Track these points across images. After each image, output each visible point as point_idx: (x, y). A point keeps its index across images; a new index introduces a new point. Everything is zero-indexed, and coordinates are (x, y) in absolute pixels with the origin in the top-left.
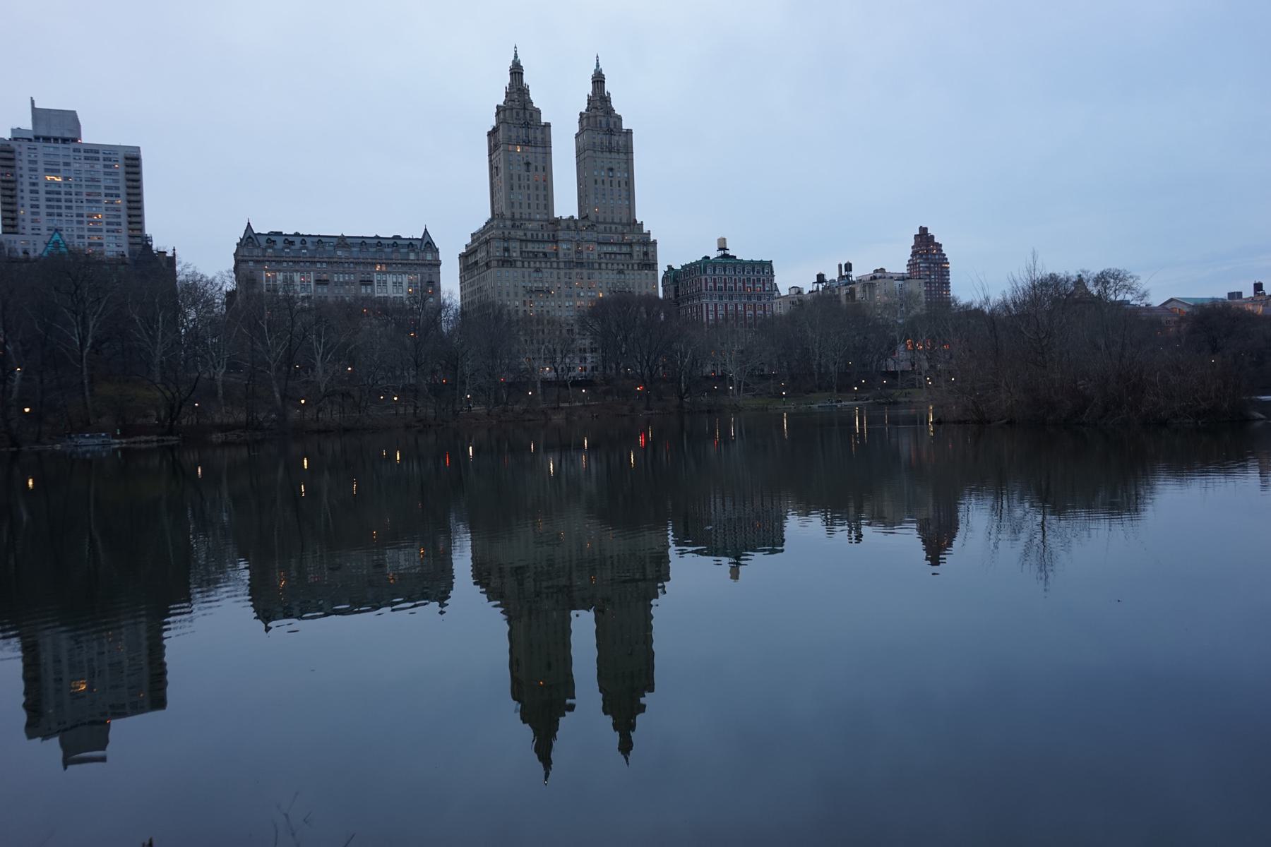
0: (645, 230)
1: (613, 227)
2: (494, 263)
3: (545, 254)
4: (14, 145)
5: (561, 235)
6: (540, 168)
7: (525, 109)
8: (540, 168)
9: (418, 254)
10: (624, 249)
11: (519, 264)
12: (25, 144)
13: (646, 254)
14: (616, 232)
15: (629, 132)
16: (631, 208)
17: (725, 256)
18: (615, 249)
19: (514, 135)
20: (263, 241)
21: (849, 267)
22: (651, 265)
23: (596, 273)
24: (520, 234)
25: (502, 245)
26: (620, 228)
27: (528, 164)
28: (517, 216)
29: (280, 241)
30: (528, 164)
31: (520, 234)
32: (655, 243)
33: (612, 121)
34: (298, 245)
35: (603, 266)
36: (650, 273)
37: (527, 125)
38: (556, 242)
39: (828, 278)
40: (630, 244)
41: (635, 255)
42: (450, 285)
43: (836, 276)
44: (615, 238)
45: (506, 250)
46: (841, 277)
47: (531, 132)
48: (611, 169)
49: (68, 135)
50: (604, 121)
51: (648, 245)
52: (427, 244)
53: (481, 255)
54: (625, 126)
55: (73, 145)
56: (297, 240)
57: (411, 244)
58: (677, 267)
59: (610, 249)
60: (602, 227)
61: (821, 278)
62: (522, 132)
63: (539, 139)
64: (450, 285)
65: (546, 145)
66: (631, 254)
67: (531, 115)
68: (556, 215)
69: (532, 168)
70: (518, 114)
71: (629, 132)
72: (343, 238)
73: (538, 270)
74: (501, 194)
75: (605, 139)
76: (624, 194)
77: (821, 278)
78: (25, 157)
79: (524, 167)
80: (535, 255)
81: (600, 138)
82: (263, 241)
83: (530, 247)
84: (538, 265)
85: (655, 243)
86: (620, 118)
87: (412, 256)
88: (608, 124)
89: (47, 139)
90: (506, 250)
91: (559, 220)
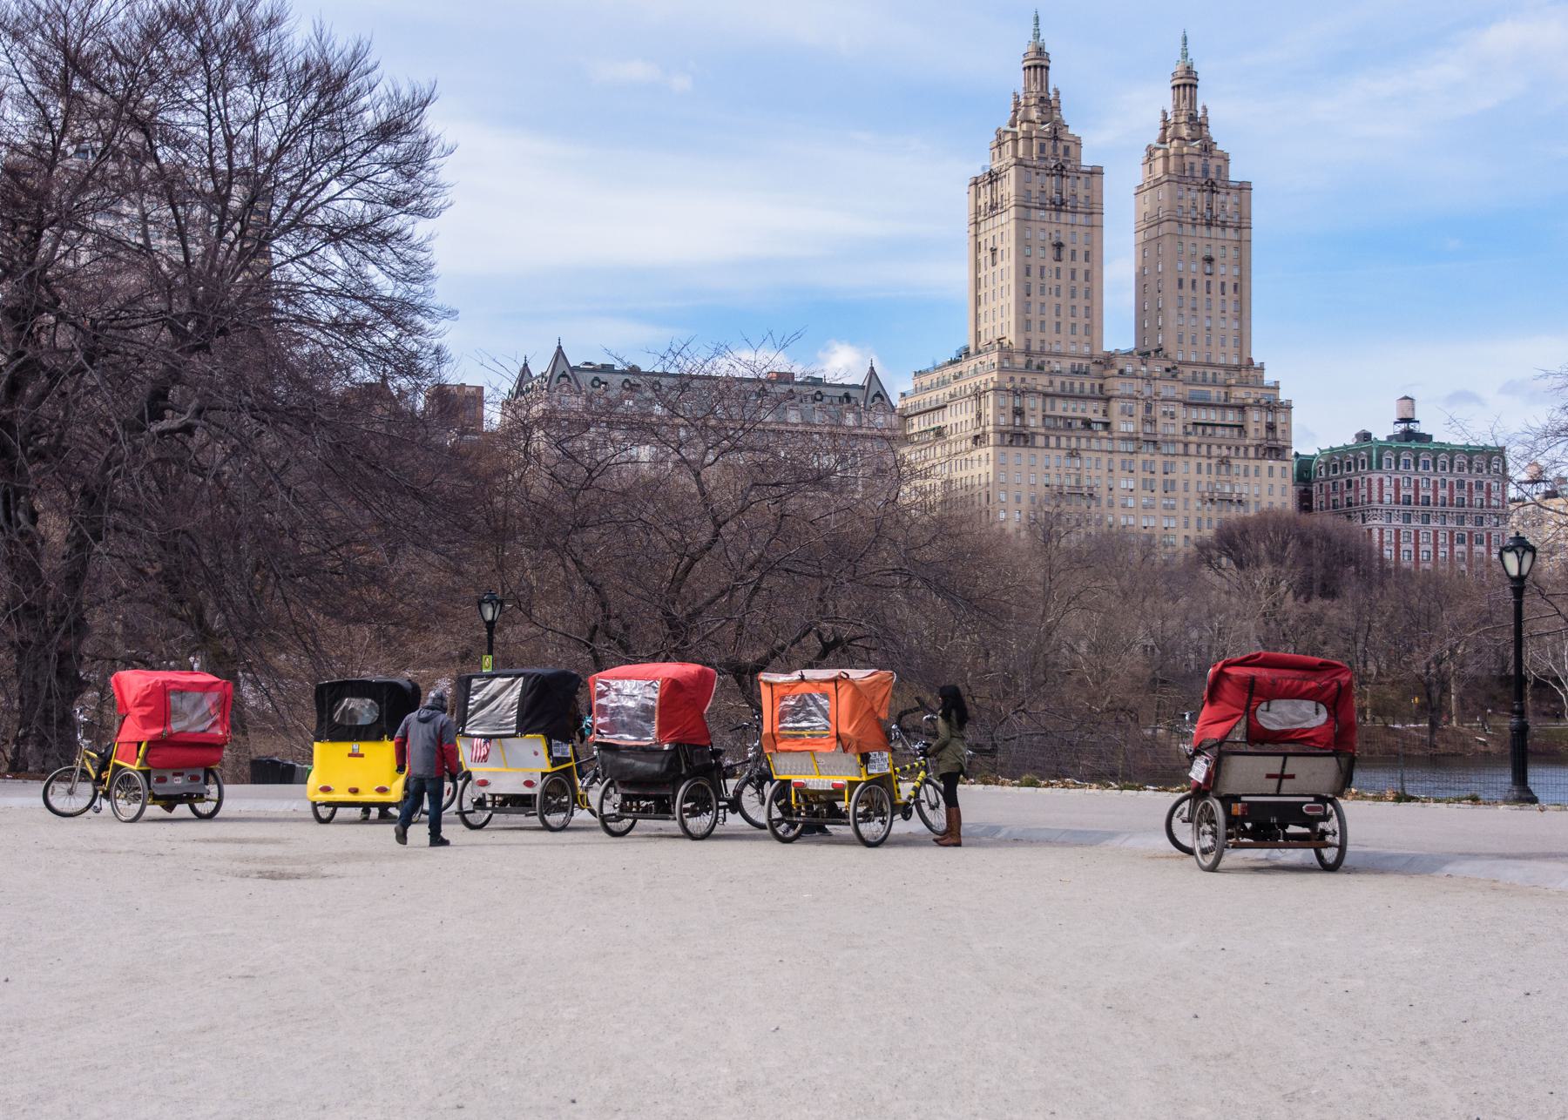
0: (1269, 378)
1: (1210, 372)
3: (1087, 424)
5: (1117, 386)
6: (1080, 256)
7: (1056, 138)
8: (1080, 256)
11: (1040, 441)
13: (1271, 427)
14: (1214, 383)
16: (1242, 340)
23: (1180, 461)
26: (1222, 375)
27: (1059, 246)
28: (1035, 347)
30: (1059, 246)
32: (1288, 407)
33: (1213, 163)
35: (1192, 449)
37: (1060, 171)
38: (1108, 399)
40: (1241, 408)
41: (1251, 429)
45: (1019, 412)
48: (1209, 260)
62: (1051, 183)
63: (1081, 198)
65: (1093, 210)
67: (1067, 149)
69: (1066, 254)
73: (1073, 454)
76: (1230, 308)
79: (1051, 252)
84: (1074, 443)
87: (850, 419)
88: (1206, 171)
90: (1019, 412)
91: (1108, 361)
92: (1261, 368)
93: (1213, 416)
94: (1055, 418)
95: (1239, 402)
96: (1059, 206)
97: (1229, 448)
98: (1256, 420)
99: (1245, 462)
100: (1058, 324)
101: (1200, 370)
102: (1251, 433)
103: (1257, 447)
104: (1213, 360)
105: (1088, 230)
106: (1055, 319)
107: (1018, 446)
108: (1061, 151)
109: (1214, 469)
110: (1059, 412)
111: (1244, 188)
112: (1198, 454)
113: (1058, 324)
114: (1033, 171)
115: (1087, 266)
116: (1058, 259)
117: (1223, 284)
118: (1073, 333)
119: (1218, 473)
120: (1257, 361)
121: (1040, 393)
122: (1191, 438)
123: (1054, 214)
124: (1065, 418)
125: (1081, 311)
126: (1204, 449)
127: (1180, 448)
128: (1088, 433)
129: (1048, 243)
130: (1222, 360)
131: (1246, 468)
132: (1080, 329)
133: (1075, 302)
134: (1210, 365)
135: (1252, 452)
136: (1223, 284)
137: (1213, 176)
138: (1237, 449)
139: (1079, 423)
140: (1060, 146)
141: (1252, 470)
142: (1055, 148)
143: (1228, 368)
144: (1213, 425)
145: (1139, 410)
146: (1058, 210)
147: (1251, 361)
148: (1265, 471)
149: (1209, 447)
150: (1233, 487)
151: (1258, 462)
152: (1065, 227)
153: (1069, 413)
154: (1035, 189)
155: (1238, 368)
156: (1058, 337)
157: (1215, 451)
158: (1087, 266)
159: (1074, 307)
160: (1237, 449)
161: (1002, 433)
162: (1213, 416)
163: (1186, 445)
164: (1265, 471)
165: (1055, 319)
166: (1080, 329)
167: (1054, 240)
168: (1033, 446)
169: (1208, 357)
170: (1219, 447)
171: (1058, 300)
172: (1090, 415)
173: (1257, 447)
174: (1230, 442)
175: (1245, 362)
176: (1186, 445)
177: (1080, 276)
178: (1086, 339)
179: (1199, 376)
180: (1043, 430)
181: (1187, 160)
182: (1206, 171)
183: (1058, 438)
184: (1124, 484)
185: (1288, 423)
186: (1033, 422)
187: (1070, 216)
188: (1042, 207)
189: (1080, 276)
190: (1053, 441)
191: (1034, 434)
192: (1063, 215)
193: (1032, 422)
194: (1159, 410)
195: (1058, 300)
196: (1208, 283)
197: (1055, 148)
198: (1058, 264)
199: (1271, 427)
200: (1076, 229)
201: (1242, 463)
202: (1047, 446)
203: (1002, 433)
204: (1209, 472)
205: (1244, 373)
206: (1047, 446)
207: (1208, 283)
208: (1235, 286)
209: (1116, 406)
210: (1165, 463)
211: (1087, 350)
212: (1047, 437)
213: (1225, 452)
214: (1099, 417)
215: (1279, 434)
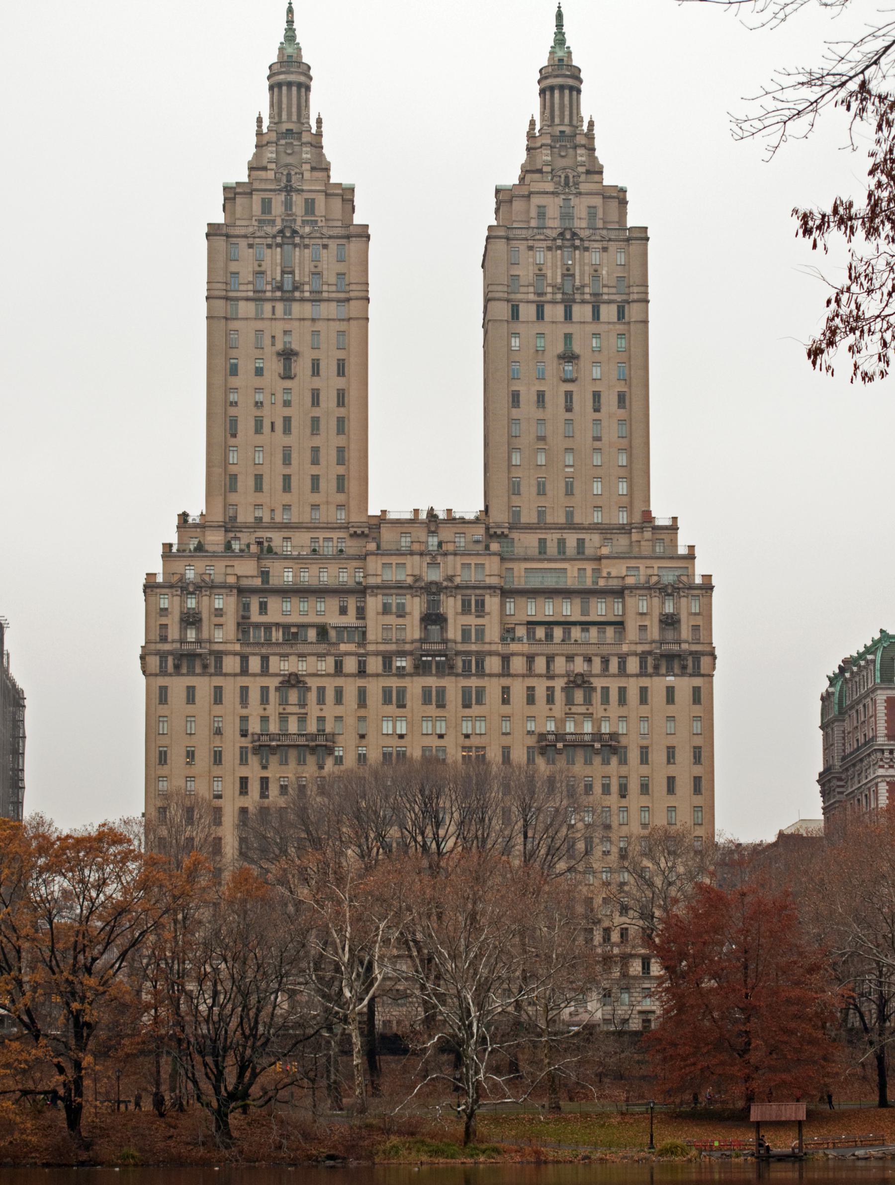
1: (571, 540)
6: (329, 367)
7: (289, 189)
8: (329, 367)
11: (231, 664)
13: (670, 622)
26: (593, 540)
27: (288, 355)
28: (245, 516)
31: (247, 569)
32: (707, 587)
35: (518, 664)
36: (684, 685)
40: (619, 593)
44: (573, 575)
50: (553, 206)
62: (273, 259)
68: (374, 510)
69: (301, 367)
70: (266, 206)
76: (611, 432)
88: (567, 215)
90: (191, 620)
92: (674, 528)
93: (568, 610)
94: (268, 627)
95: (614, 583)
96: (288, 294)
97: (589, 660)
98: (642, 610)
99: (622, 682)
100: (287, 479)
101: (552, 538)
102: (632, 631)
103: (643, 657)
104: (577, 519)
105: (343, 326)
106: (282, 470)
107: (191, 673)
108: (298, 208)
109: (559, 696)
110: (273, 616)
111: (641, 236)
112: (530, 672)
113: (287, 479)
114: (243, 243)
115: (340, 383)
116: (287, 376)
117: (597, 396)
118: (315, 488)
119: (570, 701)
120: (661, 517)
121: (231, 587)
122: (514, 647)
123: (280, 307)
124: (286, 627)
125: (329, 456)
126: (540, 664)
127: (493, 664)
128: (322, 648)
129: (269, 350)
130: (597, 518)
131: (622, 691)
132: (328, 485)
133: (317, 441)
134: (571, 526)
135: (633, 665)
136: (597, 396)
137: (580, 224)
138: (606, 662)
139: (312, 634)
140: (298, 201)
141: (633, 695)
142: (288, 205)
143: (606, 531)
144: (567, 624)
145: (416, 606)
146: (288, 299)
147: (647, 516)
148: (658, 695)
149: (550, 659)
150: (597, 723)
151: (645, 682)
152: (297, 325)
153: (295, 619)
154: (245, 269)
155: (626, 530)
156: (286, 498)
157: (560, 665)
158: (340, 383)
159: (315, 450)
160: (606, 662)
161: (163, 656)
162: (568, 610)
163: (506, 659)
164: (658, 695)
165: (282, 470)
166: (328, 485)
167: (279, 346)
168: (219, 672)
169: (570, 514)
170: (570, 658)
171: (287, 441)
172: (334, 619)
173: (643, 657)
174: (605, 650)
175: (637, 518)
176: (506, 659)
177: (328, 400)
178: (341, 498)
179: (552, 549)
180: (237, 647)
181: (536, 200)
182: (567, 215)
183: (265, 659)
184: (387, 728)
185: (706, 614)
186: (223, 635)
187: (308, 306)
188: (258, 298)
189: (328, 400)
190: (255, 664)
191: (219, 656)
192: (296, 308)
193: (218, 635)
194: (450, 606)
195: (287, 441)
196: (569, 395)
197: (288, 205)
198: (288, 384)
199: (670, 622)
200: (320, 326)
201: (614, 685)
202: (244, 671)
203: (163, 656)
204: (550, 700)
205: (635, 536)
206: (244, 671)
207: (569, 395)
208: (622, 399)
209: (373, 603)
210: (466, 691)
211: (342, 516)
212: (244, 659)
213: (580, 666)
214: (350, 619)
215: (685, 632)
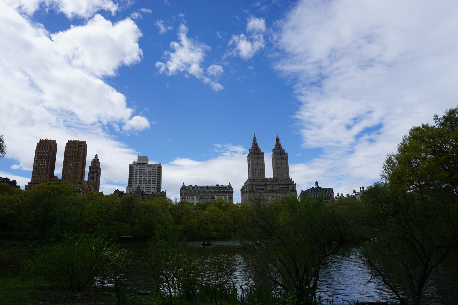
2: (248, 192)
4: (133, 166)
9: (228, 190)
10: (286, 186)
12: (135, 165)
13: (293, 187)
15: (287, 153)
17: (318, 187)
18: (284, 186)
19: (254, 156)
20: (187, 188)
21: (363, 188)
22: (295, 191)
24: (256, 183)
25: (250, 186)
27: (258, 164)
29: (191, 187)
32: (295, 184)
34: (196, 189)
37: (257, 154)
39: (357, 191)
40: (288, 185)
42: (237, 199)
43: (359, 191)
44: (283, 183)
45: (252, 188)
46: (361, 191)
47: (258, 155)
49: (145, 162)
51: (293, 186)
52: (230, 187)
53: (245, 189)
54: (285, 152)
55: (146, 165)
56: (196, 187)
57: (225, 187)
58: (304, 191)
59: (282, 186)
60: (279, 180)
61: (354, 192)
62: (256, 156)
64: (237, 199)
66: (288, 188)
68: (266, 178)
69: (259, 165)
71: (287, 153)
72: (207, 186)
74: (250, 173)
75: (280, 156)
77: (354, 192)
78: (135, 168)
79: (256, 165)
80: (260, 189)
81: (279, 156)
82: (187, 188)
83: (258, 187)
85: (295, 184)
86: (284, 150)
89: (140, 164)
90: (252, 188)
91: (267, 179)
